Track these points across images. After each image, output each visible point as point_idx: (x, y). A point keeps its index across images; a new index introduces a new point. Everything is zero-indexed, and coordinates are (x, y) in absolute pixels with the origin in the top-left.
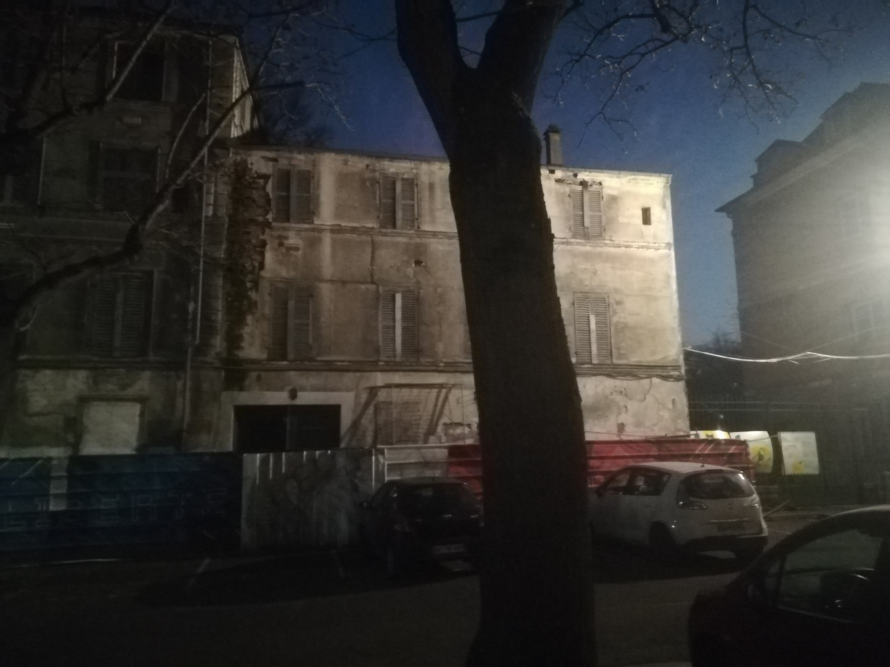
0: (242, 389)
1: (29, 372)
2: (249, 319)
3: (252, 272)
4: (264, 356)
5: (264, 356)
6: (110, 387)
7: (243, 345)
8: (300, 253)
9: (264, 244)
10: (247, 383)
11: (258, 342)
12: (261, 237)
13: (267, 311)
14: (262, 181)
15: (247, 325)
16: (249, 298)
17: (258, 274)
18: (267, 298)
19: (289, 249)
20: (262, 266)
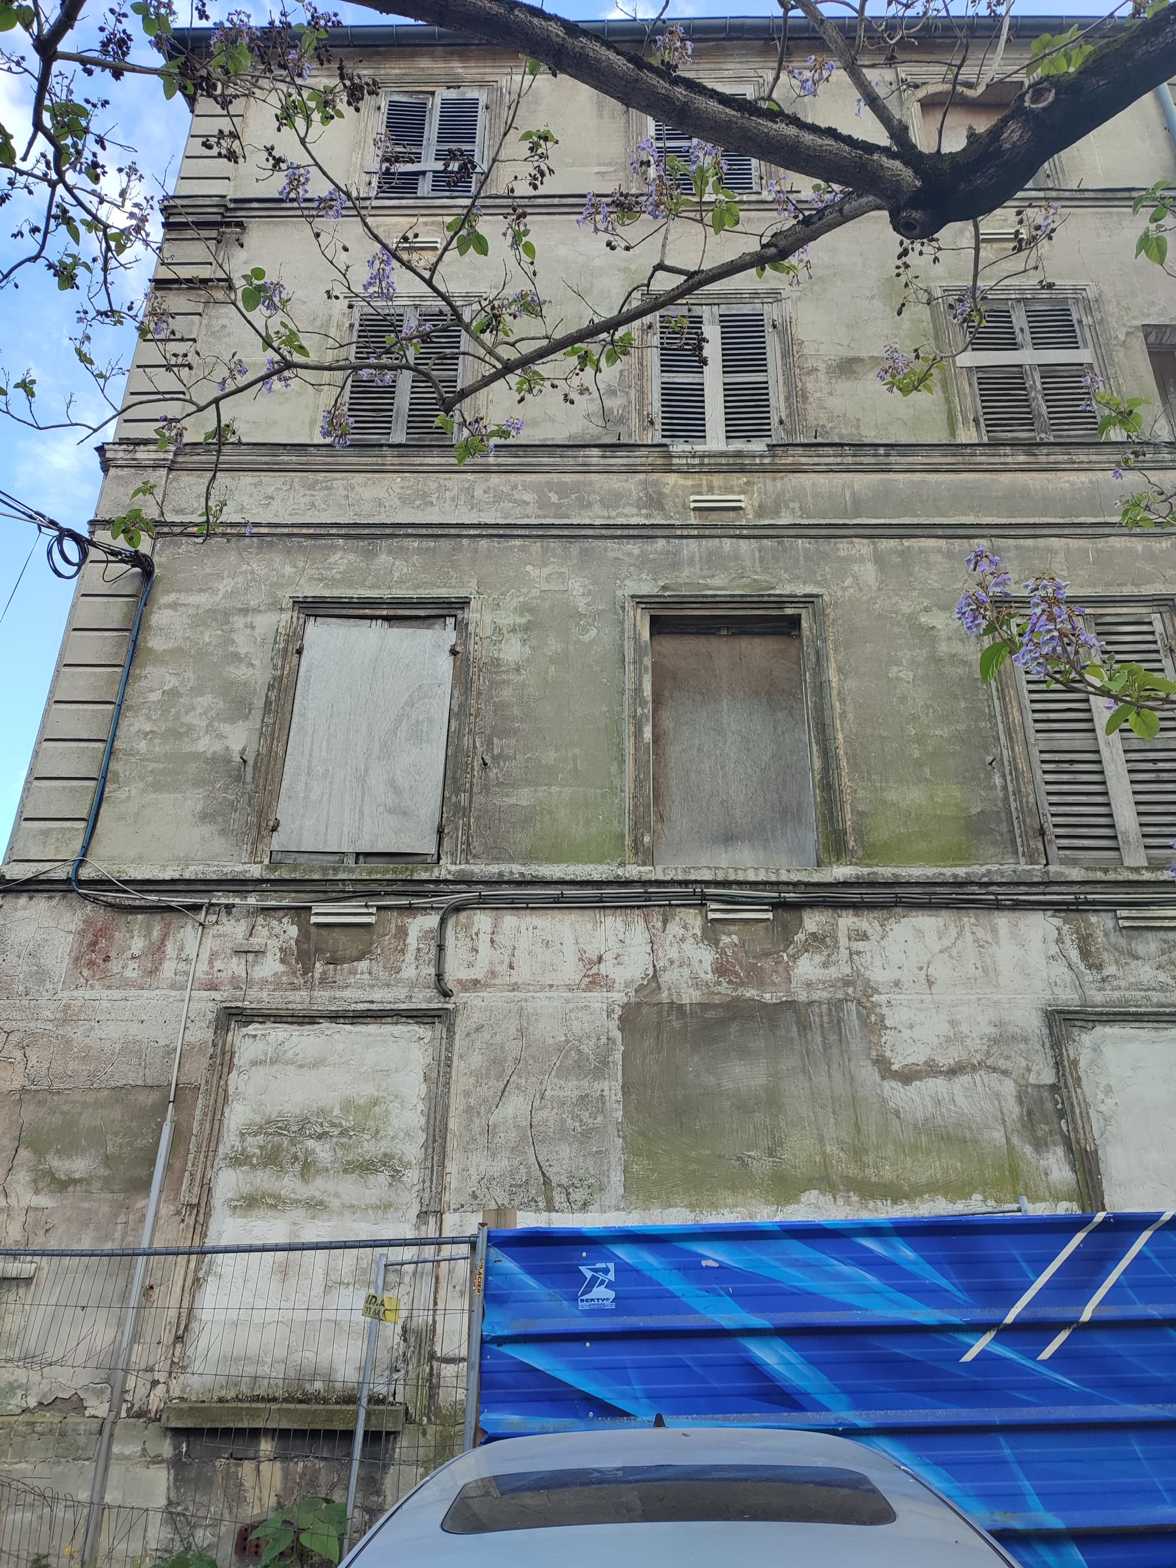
1: (866, 922)
6: (1146, 973)
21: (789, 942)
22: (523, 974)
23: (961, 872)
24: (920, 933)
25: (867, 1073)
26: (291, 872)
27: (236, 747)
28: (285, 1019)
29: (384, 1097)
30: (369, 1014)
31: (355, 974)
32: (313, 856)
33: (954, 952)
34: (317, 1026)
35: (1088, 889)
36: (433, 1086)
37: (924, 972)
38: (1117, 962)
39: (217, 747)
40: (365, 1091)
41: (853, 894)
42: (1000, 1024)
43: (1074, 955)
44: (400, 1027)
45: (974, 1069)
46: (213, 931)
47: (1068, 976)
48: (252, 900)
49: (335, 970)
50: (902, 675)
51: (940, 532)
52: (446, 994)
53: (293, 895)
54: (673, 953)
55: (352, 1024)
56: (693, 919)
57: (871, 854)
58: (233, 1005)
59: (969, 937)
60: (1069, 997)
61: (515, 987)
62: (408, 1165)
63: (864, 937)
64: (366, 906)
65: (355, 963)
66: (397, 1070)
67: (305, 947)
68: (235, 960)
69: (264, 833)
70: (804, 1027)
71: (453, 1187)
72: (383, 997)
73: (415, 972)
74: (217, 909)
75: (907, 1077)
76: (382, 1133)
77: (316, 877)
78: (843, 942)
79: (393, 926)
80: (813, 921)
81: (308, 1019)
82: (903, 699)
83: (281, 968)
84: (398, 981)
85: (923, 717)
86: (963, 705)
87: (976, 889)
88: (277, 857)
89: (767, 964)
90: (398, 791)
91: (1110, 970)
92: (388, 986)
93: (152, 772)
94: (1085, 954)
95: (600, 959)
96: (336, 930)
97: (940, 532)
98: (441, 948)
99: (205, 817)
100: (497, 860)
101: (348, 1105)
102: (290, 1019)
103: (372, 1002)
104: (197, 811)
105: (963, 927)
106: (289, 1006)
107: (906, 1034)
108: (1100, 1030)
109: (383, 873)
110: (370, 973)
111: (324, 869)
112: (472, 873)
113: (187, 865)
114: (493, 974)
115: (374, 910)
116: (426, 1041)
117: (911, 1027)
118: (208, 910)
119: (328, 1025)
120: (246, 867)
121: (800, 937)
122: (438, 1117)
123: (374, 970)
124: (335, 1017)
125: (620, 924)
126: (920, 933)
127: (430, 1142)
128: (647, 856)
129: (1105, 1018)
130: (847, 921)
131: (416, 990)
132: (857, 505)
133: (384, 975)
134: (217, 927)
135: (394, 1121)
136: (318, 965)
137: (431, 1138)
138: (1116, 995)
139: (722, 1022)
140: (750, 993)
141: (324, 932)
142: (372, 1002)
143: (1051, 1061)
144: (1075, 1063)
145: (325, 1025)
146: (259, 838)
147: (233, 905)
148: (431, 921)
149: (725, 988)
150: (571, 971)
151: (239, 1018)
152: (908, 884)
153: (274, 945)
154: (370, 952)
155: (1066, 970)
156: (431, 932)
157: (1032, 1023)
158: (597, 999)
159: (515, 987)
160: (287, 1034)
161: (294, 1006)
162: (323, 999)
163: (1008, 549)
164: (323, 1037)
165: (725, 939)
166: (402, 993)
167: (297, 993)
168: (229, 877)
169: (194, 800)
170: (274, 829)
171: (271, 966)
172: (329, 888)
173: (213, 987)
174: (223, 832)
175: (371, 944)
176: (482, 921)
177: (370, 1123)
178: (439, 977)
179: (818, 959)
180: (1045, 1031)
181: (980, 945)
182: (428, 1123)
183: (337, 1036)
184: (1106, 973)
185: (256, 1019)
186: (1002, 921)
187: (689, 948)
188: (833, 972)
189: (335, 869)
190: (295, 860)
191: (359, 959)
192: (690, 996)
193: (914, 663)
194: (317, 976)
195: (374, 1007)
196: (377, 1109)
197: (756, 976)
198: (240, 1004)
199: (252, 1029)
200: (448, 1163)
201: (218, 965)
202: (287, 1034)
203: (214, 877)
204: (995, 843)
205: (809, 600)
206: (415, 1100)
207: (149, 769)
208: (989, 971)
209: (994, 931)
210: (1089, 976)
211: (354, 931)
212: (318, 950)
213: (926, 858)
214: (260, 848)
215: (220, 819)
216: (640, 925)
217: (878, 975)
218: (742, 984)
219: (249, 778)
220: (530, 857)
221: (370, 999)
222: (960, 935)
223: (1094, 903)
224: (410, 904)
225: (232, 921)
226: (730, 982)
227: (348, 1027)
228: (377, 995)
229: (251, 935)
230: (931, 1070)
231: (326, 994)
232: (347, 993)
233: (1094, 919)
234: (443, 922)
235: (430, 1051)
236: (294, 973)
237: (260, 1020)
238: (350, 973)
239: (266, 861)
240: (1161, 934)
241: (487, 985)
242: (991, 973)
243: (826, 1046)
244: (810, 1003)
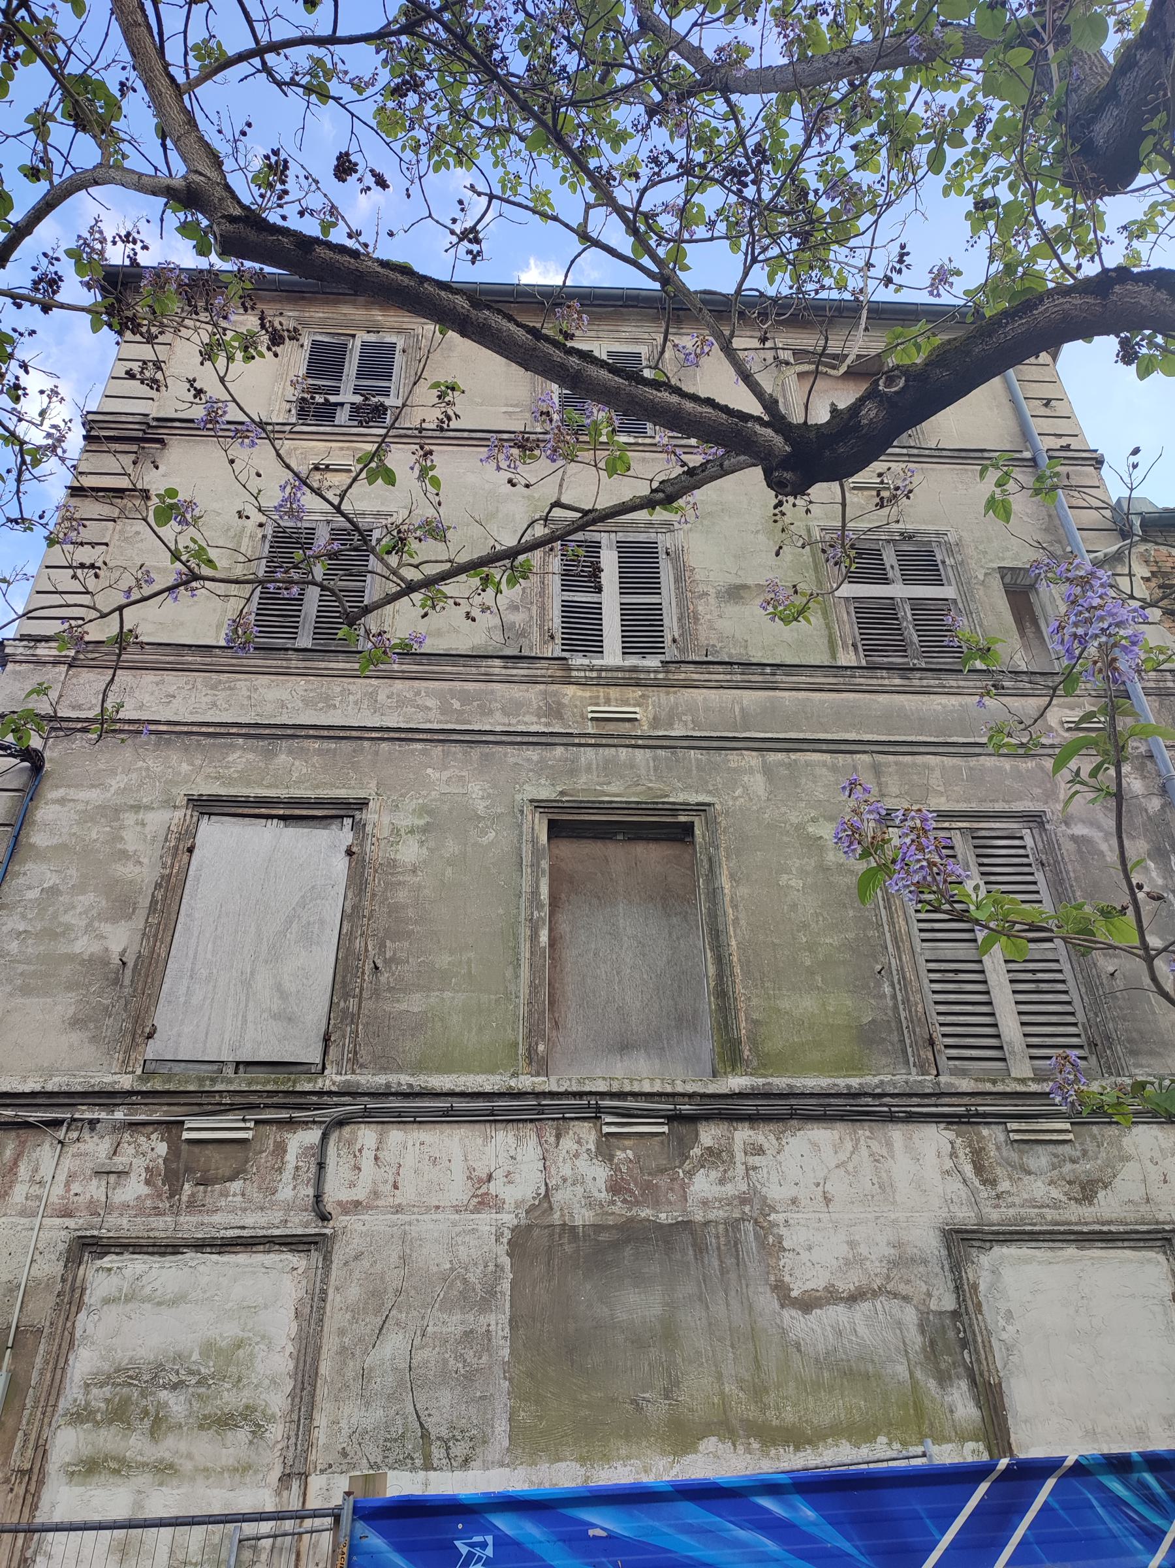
1: (762, 1135)
6: (1038, 1188)
21: (685, 1157)
22: (408, 1194)
23: (855, 1082)
24: (815, 1146)
25: (767, 1301)
26: (164, 1083)
27: (116, 948)
28: (145, 1249)
29: (249, 1339)
30: (239, 1241)
31: (227, 1196)
32: (190, 1066)
33: (850, 1167)
34: (180, 1257)
35: (978, 1100)
36: (305, 1324)
37: (820, 1188)
38: (1010, 1178)
39: (95, 948)
40: (231, 1330)
41: (749, 1107)
42: (898, 1245)
43: (968, 1169)
44: (272, 1255)
45: (875, 1294)
46: (72, 1149)
47: (964, 1192)
48: (119, 1115)
49: (205, 1192)
50: (792, 883)
51: (824, 747)
52: (324, 1217)
53: (165, 1108)
54: (566, 1171)
55: (219, 1253)
56: (586, 1133)
57: (766, 1063)
58: (88, 1233)
59: (864, 1152)
61: (398, 1209)
62: (271, 1419)
63: (760, 1151)
64: (244, 1120)
65: (227, 1184)
66: (266, 1307)
67: (174, 1166)
68: (95, 1182)
69: (139, 1040)
70: (700, 1249)
71: (320, 1443)
72: (255, 1222)
73: (292, 1193)
74: (80, 1124)
75: (807, 1304)
76: (245, 1381)
77: (191, 1088)
78: (739, 1156)
79: (271, 1142)
80: (709, 1135)
81: (170, 1248)
82: (794, 907)
83: (145, 1190)
85: (813, 925)
86: (851, 913)
87: (869, 1100)
88: (151, 1067)
89: (662, 1181)
90: (283, 995)
91: (1004, 1185)
92: (262, 1209)
93: (21, 974)
94: (979, 1169)
95: (490, 1177)
96: (210, 1147)
97: (824, 747)
98: (321, 1166)
99: (76, 1023)
100: (384, 1069)
101: (209, 1349)
102: (150, 1249)
103: (243, 1228)
104: (68, 1016)
105: (858, 1140)
106: (151, 1234)
107: (805, 1256)
108: (999, 1251)
109: (264, 1084)
110: (243, 1195)
111: (201, 1080)
112: (358, 1084)
113: (51, 1076)
114: (376, 1194)
115: (251, 1125)
116: (300, 1271)
117: (810, 1248)
118: (69, 1125)
119: (193, 1255)
120: (116, 1077)
121: (696, 1151)
122: (309, 1360)
123: (247, 1192)
124: (200, 1246)
125: (511, 1139)
126: (815, 1146)
127: (298, 1391)
128: (541, 1066)
129: (1001, 1237)
130: (743, 1134)
131: (292, 1213)
132: (746, 719)
133: (257, 1197)
134: (78, 1145)
135: (260, 1367)
136: (186, 1186)
137: (299, 1386)
138: (1011, 1212)
139: (615, 1245)
140: (645, 1213)
141: (196, 1149)
142: (243, 1228)
143: (951, 1285)
144: (975, 1287)
145: (190, 1255)
146: (133, 1045)
147: (98, 1120)
148: (313, 1136)
149: (619, 1208)
150: (458, 1191)
151: (94, 1249)
152: (803, 1095)
153: (139, 1164)
154: (245, 1171)
155: (961, 1186)
156: (312, 1148)
157: (930, 1243)
158: (485, 1221)
159: (398, 1209)
160: (145, 1267)
161: (157, 1234)
162: (190, 1225)
163: (888, 765)
164: (186, 1269)
165: (620, 1155)
166: (277, 1216)
167: (161, 1218)
168: (97, 1089)
169: (65, 1004)
170: (150, 1036)
171: (134, 1189)
172: (205, 1100)
173: (67, 1213)
174: (94, 1039)
175: (247, 1162)
176: (367, 1135)
177: (233, 1369)
178: (318, 1198)
179: (714, 1175)
180: (944, 1252)
182: (296, 1367)
183: (201, 1268)
184: (1000, 1189)
185: (113, 1249)
186: (897, 1133)
187: (583, 1164)
188: (729, 1190)
189: (213, 1080)
190: (170, 1069)
191: (231, 1179)
192: (583, 1217)
193: (802, 872)
194: (184, 1198)
195: (245, 1233)
196: (241, 1352)
197: (650, 1194)
198: (96, 1233)
199: (108, 1261)
200: (316, 1415)
201: (76, 1187)
202: (145, 1267)
203: (80, 1089)
204: (886, 1053)
205: (701, 808)
206: (284, 1341)
207: (19, 971)
208: (885, 1187)
209: (889, 1144)
210: (984, 1192)
211: (228, 1148)
212: (188, 1170)
213: (820, 1069)
214: (133, 1057)
215: (92, 1026)
217: (775, 1192)
218: (637, 1203)
219: (127, 982)
220: (419, 1067)
221: (241, 1224)
222: (855, 1148)
224: (291, 1118)
225: (96, 1137)
226: (625, 1201)
228: (249, 1220)
229: (115, 1153)
230: (831, 1296)
231: (194, 1219)
232: (217, 1218)
235: (304, 1283)
236: (159, 1196)
237: (117, 1250)
238: (221, 1195)
239: (139, 1071)
240: (1051, 1148)
241: (369, 1207)
242: (888, 1190)
243: (724, 1271)
244: (707, 1223)
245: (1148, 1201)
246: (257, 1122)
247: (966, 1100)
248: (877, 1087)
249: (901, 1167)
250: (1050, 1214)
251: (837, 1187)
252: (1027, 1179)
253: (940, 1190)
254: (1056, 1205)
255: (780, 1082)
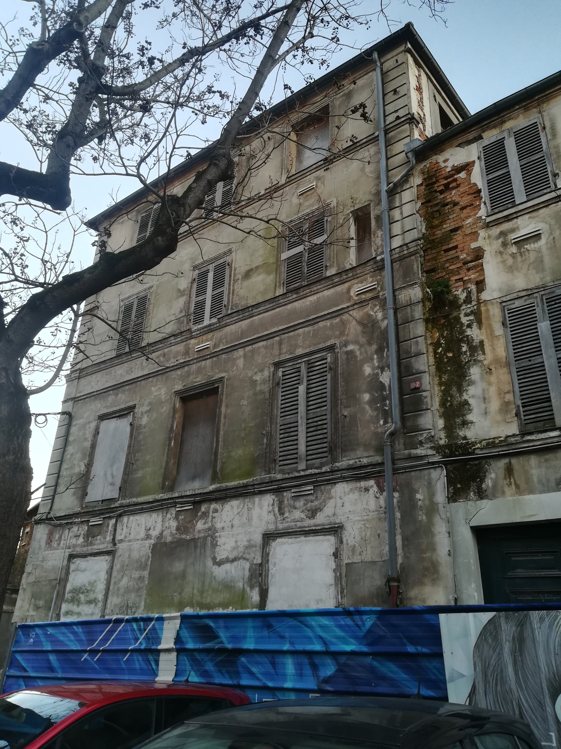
0: (481, 495)
2: (475, 372)
3: (468, 300)
4: (513, 429)
5: (513, 429)
6: (297, 514)
7: (470, 417)
8: (543, 242)
9: (479, 254)
10: (489, 483)
11: (495, 405)
12: (473, 245)
13: (501, 352)
14: (463, 175)
15: (471, 383)
16: (469, 341)
17: (478, 299)
18: (499, 330)
19: (519, 243)
20: (481, 285)
21: (197, 516)
35: (281, 482)
43: (276, 509)
59: (246, 507)
60: (272, 527)
61: (130, 541)
63: (216, 511)
78: (211, 514)
84: (106, 541)
91: (287, 515)
94: (280, 509)
95: (150, 529)
114: (126, 537)
121: (200, 514)
125: (156, 516)
130: (213, 506)
140: (184, 536)
150: (142, 534)
155: (273, 516)
159: (130, 541)
165: (180, 517)
166: (105, 545)
179: (203, 521)
181: (249, 509)
184: (285, 516)
188: (206, 526)
208: (250, 520)
210: (280, 518)
216: (160, 516)
217: (219, 525)
218: (182, 533)
222: (244, 506)
223: (284, 488)
226: (179, 533)
227: (93, 558)
233: (285, 494)
234: (116, 521)
240: (305, 498)
241: (125, 541)
244: (199, 538)
245: (334, 515)
246: (104, 518)
247: (277, 483)
248: (252, 482)
249: (256, 512)
250: (299, 524)
251: (236, 522)
252: (294, 511)
253: (266, 519)
254: (302, 520)
255: (224, 485)
